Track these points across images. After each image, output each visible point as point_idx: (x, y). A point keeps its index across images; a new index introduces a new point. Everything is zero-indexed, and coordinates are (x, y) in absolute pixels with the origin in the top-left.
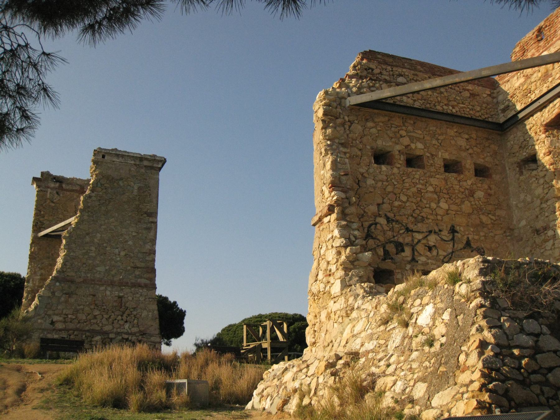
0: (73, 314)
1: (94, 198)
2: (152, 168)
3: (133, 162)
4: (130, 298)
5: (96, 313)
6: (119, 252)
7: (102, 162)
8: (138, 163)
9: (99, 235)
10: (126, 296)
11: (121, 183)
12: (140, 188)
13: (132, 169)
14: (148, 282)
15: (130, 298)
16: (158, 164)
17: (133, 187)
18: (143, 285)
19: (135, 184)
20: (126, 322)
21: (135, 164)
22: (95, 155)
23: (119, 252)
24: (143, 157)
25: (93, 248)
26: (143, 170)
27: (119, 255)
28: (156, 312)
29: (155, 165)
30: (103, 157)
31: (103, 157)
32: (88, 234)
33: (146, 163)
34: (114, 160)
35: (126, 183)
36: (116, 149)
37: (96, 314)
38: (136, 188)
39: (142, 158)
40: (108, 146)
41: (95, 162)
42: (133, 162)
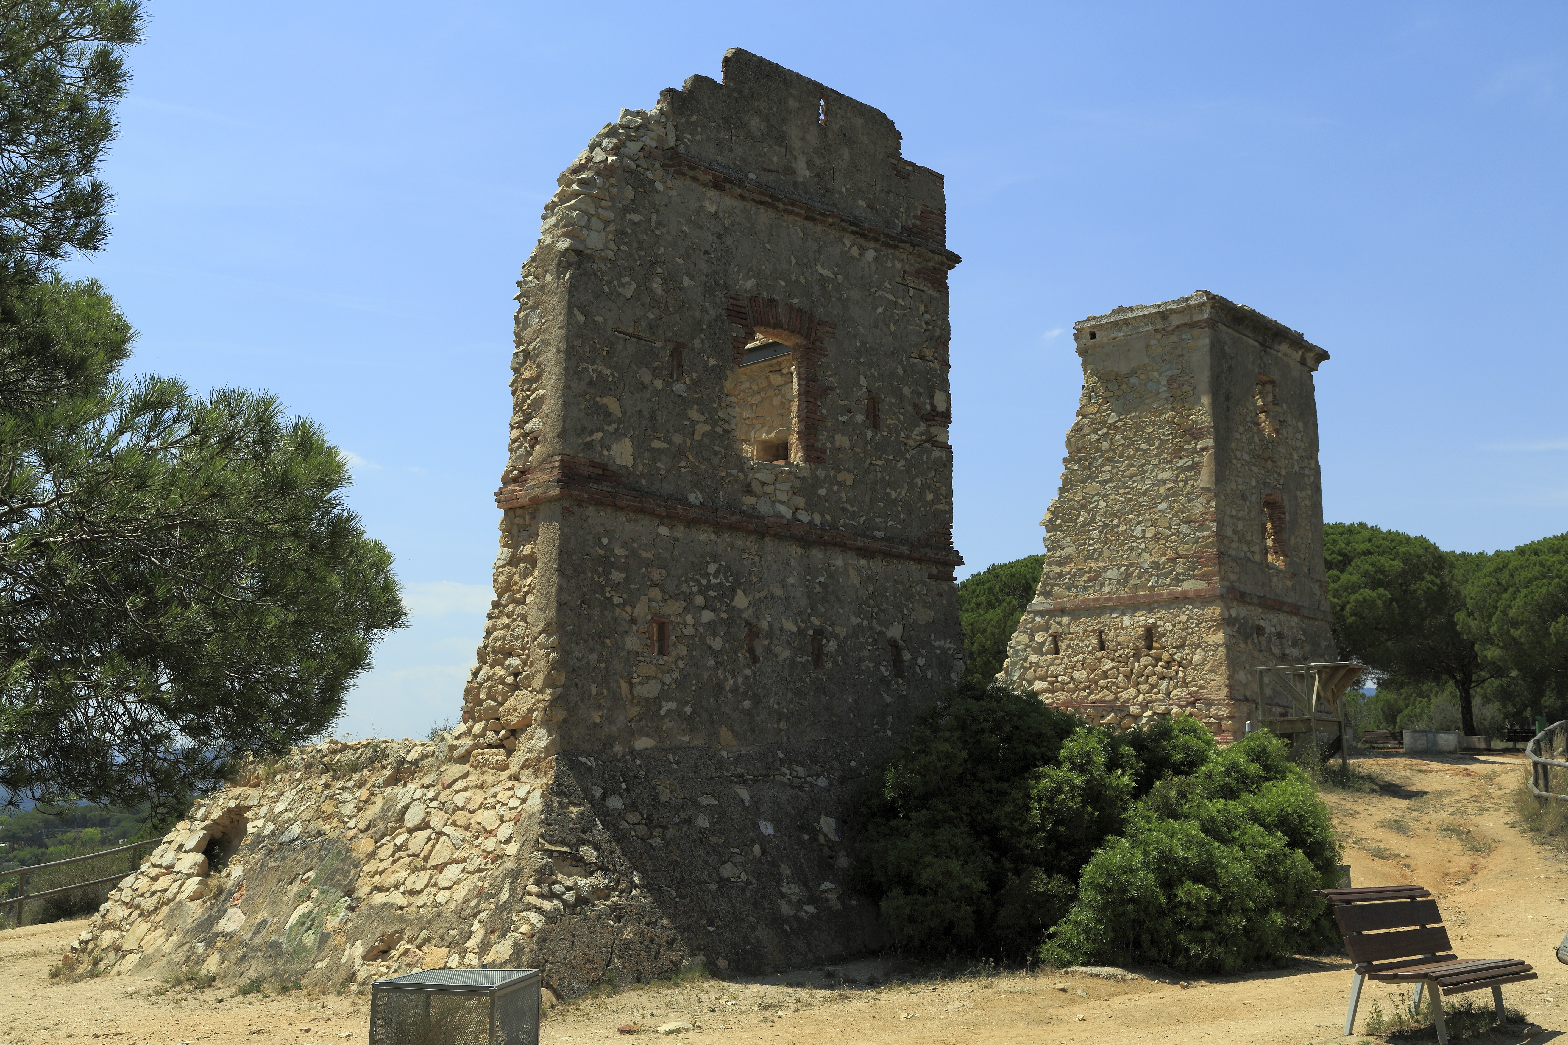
0: (1064, 675)
1: (1086, 430)
2: (1193, 325)
3: (1150, 328)
4: (1169, 626)
5: (1107, 665)
6: (1144, 531)
7: (1094, 347)
8: (1159, 326)
9: (1102, 504)
10: (1159, 623)
11: (1133, 380)
12: (1171, 380)
13: (1153, 342)
14: (1202, 585)
15: (1169, 626)
16: (1202, 312)
17: (1158, 382)
18: (1191, 594)
19: (1160, 375)
20: (1163, 678)
21: (1156, 331)
22: (1077, 337)
23: (1144, 531)
24: (1163, 308)
25: (1095, 534)
26: (1174, 338)
27: (1144, 537)
28: (1222, 650)
29: (1197, 318)
30: (1093, 336)
31: (1093, 336)
32: (1083, 507)
33: (1175, 320)
34: (1113, 335)
35: (1142, 377)
36: (1121, 310)
37: (1107, 667)
38: (1164, 382)
39: (1163, 314)
40: (1103, 308)
41: (1082, 352)
42: (1150, 328)
